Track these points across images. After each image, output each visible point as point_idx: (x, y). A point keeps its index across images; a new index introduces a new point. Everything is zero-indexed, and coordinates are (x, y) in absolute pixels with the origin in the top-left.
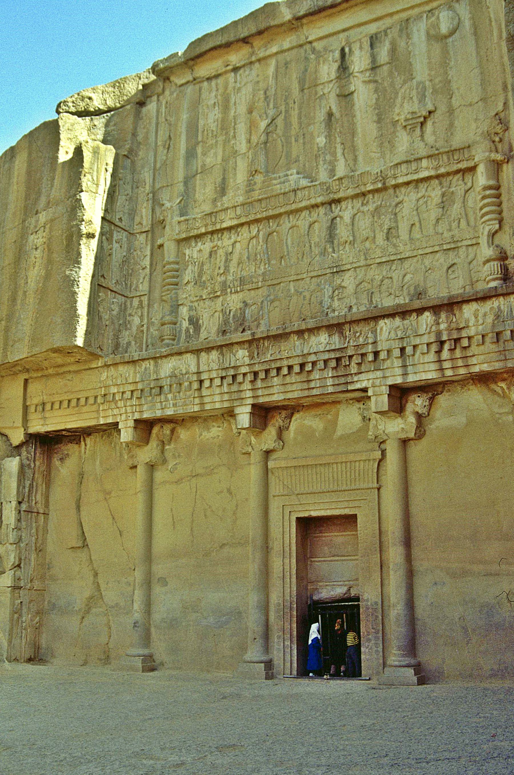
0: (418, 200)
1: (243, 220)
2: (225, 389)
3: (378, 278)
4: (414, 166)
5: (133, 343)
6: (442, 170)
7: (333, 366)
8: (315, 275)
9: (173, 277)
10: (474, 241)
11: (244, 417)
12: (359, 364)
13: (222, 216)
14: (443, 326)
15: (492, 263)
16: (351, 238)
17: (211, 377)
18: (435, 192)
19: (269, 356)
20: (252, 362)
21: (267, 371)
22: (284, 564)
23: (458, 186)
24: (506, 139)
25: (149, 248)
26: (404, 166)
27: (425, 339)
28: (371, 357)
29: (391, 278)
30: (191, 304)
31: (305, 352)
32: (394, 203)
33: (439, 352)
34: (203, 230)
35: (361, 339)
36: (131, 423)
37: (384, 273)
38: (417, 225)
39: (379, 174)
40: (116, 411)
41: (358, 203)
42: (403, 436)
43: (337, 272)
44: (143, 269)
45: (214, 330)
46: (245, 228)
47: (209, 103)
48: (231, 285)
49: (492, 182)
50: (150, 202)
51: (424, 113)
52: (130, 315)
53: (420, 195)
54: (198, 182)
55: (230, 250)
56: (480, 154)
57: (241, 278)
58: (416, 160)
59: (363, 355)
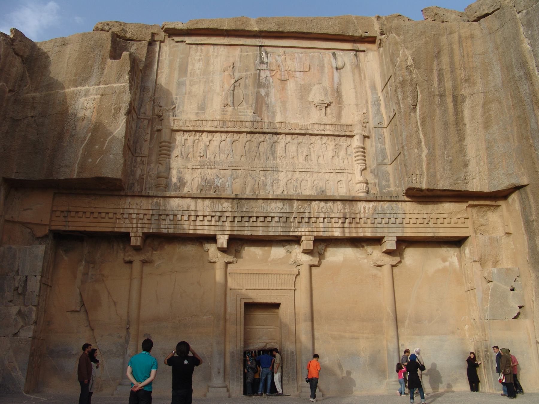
0: (322, 144)
2: (213, 223)
3: (300, 179)
5: (136, 185)
6: (337, 133)
9: (168, 150)
11: (223, 241)
14: (347, 211)
15: (362, 184)
16: (285, 155)
21: (242, 217)
22: (236, 330)
24: (367, 127)
25: (150, 129)
27: (337, 215)
28: (307, 220)
34: (191, 128)
35: (302, 209)
36: (141, 234)
37: (303, 177)
38: (322, 157)
40: (130, 225)
41: (289, 138)
42: (312, 263)
44: (146, 141)
45: (195, 187)
46: (218, 134)
47: (196, 58)
48: (208, 164)
49: (362, 145)
50: (152, 102)
51: (328, 103)
52: (134, 167)
54: (186, 100)
55: (208, 144)
56: (358, 130)
59: (302, 218)
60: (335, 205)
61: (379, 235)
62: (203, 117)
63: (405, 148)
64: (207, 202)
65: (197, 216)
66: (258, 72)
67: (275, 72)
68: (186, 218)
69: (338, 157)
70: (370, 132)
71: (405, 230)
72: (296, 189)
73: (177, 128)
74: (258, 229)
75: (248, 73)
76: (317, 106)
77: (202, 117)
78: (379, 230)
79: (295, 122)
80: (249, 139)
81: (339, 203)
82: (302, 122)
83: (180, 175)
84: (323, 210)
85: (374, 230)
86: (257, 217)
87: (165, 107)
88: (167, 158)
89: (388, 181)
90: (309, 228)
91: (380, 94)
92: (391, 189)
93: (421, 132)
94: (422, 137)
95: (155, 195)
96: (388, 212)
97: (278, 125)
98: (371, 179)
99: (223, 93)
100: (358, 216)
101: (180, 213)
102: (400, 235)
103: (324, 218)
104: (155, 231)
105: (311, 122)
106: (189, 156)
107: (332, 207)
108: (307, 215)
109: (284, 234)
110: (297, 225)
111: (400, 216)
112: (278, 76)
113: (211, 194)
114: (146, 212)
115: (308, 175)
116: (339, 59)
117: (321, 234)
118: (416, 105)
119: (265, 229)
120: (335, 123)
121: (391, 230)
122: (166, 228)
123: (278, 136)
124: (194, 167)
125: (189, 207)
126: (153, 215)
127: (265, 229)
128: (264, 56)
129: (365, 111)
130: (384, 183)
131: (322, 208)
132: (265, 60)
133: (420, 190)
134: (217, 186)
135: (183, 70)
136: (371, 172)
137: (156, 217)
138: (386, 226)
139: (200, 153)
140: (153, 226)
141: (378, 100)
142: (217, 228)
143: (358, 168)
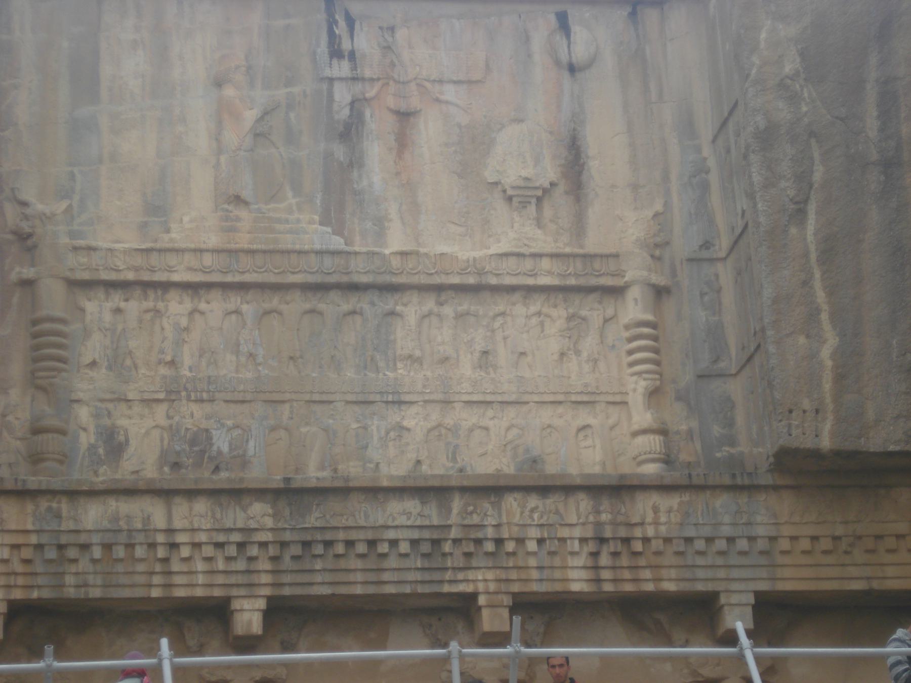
1: (216, 278)
4: (528, 264)
6: (572, 281)
7: (425, 552)
8: (355, 400)
10: (618, 398)
11: (249, 616)
12: (468, 555)
13: (172, 260)
15: (652, 437)
17: (197, 540)
18: (559, 313)
19: (313, 520)
20: (280, 525)
21: (306, 544)
23: (593, 311)
26: (512, 261)
27: (577, 532)
28: (490, 547)
29: (487, 429)
30: (99, 404)
31: (381, 522)
32: (491, 314)
33: (595, 555)
34: (130, 276)
35: (475, 516)
39: (471, 263)
43: (393, 402)
46: (216, 294)
48: (188, 386)
49: (649, 317)
51: (547, 185)
53: (533, 309)
55: (184, 322)
56: (636, 270)
57: (209, 377)
58: (534, 256)
59: (478, 542)
60: (571, 501)
61: (700, 587)
62: (166, 237)
63: (770, 333)
64: (201, 506)
65: (174, 546)
66: (325, 86)
67: (377, 86)
68: (140, 552)
69: (578, 353)
70: (674, 274)
71: (780, 573)
72: (454, 453)
73: (86, 276)
74: (351, 577)
75: (296, 90)
76: (510, 199)
77: (165, 241)
78: (701, 574)
79: (445, 249)
80: (308, 306)
81: (582, 496)
82: (465, 251)
83: (107, 422)
84: (536, 516)
85: (688, 574)
86: (350, 544)
87: (40, 207)
88: (60, 370)
89: (730, 423)
90: (498, 572)
91: (706, 151)
92: (739, 449)
93: (817, 284)
94: (821, 296)
95: (44, 487)
96: (727, 519)
97: (396, 262)
98: (680, 420)
99: (223, 159)
100: (638, 533)
101: (122, 538)
102: (763, 586)
103: (540, 541)
104: (46, 594)
105: (492, 251)
106: (128, 362)
107: (561, 507)
108: (490, 532)
109: (427, 589)
110: (460, 562)
111: (761, 531)
112: (391, 102)
113: (206, 477)
114: (20, 540)
115: (490, 413)
116: (579, 33)
117: (535, 587)
118: (806, 201)
119: (372, 577)
120: (568, 250)
121: (736, 573)
122: (83, 581)
123: (397, 296)
124: (146, 396)
125: (147, 520)
126: (39, 547)
127: (372, 577)
128: (341, 28)
129: (658, 207)
130: (717, 430)
131: (533, 511)
132: (346, 45)
133: (816, 454)
134: (220, 452)
135: (86, 80)
136: (678, 398)
137: (51, 554)
138: (720, 561)
139: (162, 352)
140: (40, 581)
141: (702, 169)
142: (233, 580)
143: (637, 387)
